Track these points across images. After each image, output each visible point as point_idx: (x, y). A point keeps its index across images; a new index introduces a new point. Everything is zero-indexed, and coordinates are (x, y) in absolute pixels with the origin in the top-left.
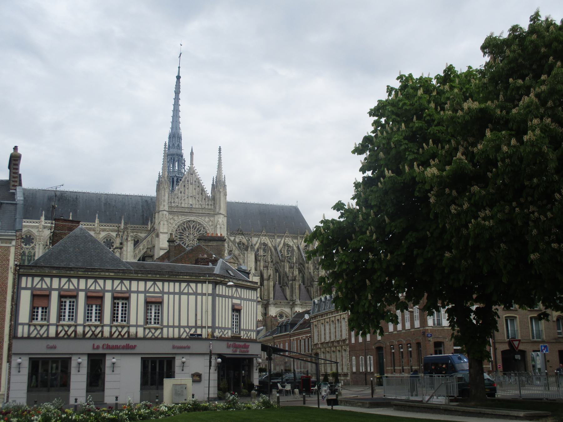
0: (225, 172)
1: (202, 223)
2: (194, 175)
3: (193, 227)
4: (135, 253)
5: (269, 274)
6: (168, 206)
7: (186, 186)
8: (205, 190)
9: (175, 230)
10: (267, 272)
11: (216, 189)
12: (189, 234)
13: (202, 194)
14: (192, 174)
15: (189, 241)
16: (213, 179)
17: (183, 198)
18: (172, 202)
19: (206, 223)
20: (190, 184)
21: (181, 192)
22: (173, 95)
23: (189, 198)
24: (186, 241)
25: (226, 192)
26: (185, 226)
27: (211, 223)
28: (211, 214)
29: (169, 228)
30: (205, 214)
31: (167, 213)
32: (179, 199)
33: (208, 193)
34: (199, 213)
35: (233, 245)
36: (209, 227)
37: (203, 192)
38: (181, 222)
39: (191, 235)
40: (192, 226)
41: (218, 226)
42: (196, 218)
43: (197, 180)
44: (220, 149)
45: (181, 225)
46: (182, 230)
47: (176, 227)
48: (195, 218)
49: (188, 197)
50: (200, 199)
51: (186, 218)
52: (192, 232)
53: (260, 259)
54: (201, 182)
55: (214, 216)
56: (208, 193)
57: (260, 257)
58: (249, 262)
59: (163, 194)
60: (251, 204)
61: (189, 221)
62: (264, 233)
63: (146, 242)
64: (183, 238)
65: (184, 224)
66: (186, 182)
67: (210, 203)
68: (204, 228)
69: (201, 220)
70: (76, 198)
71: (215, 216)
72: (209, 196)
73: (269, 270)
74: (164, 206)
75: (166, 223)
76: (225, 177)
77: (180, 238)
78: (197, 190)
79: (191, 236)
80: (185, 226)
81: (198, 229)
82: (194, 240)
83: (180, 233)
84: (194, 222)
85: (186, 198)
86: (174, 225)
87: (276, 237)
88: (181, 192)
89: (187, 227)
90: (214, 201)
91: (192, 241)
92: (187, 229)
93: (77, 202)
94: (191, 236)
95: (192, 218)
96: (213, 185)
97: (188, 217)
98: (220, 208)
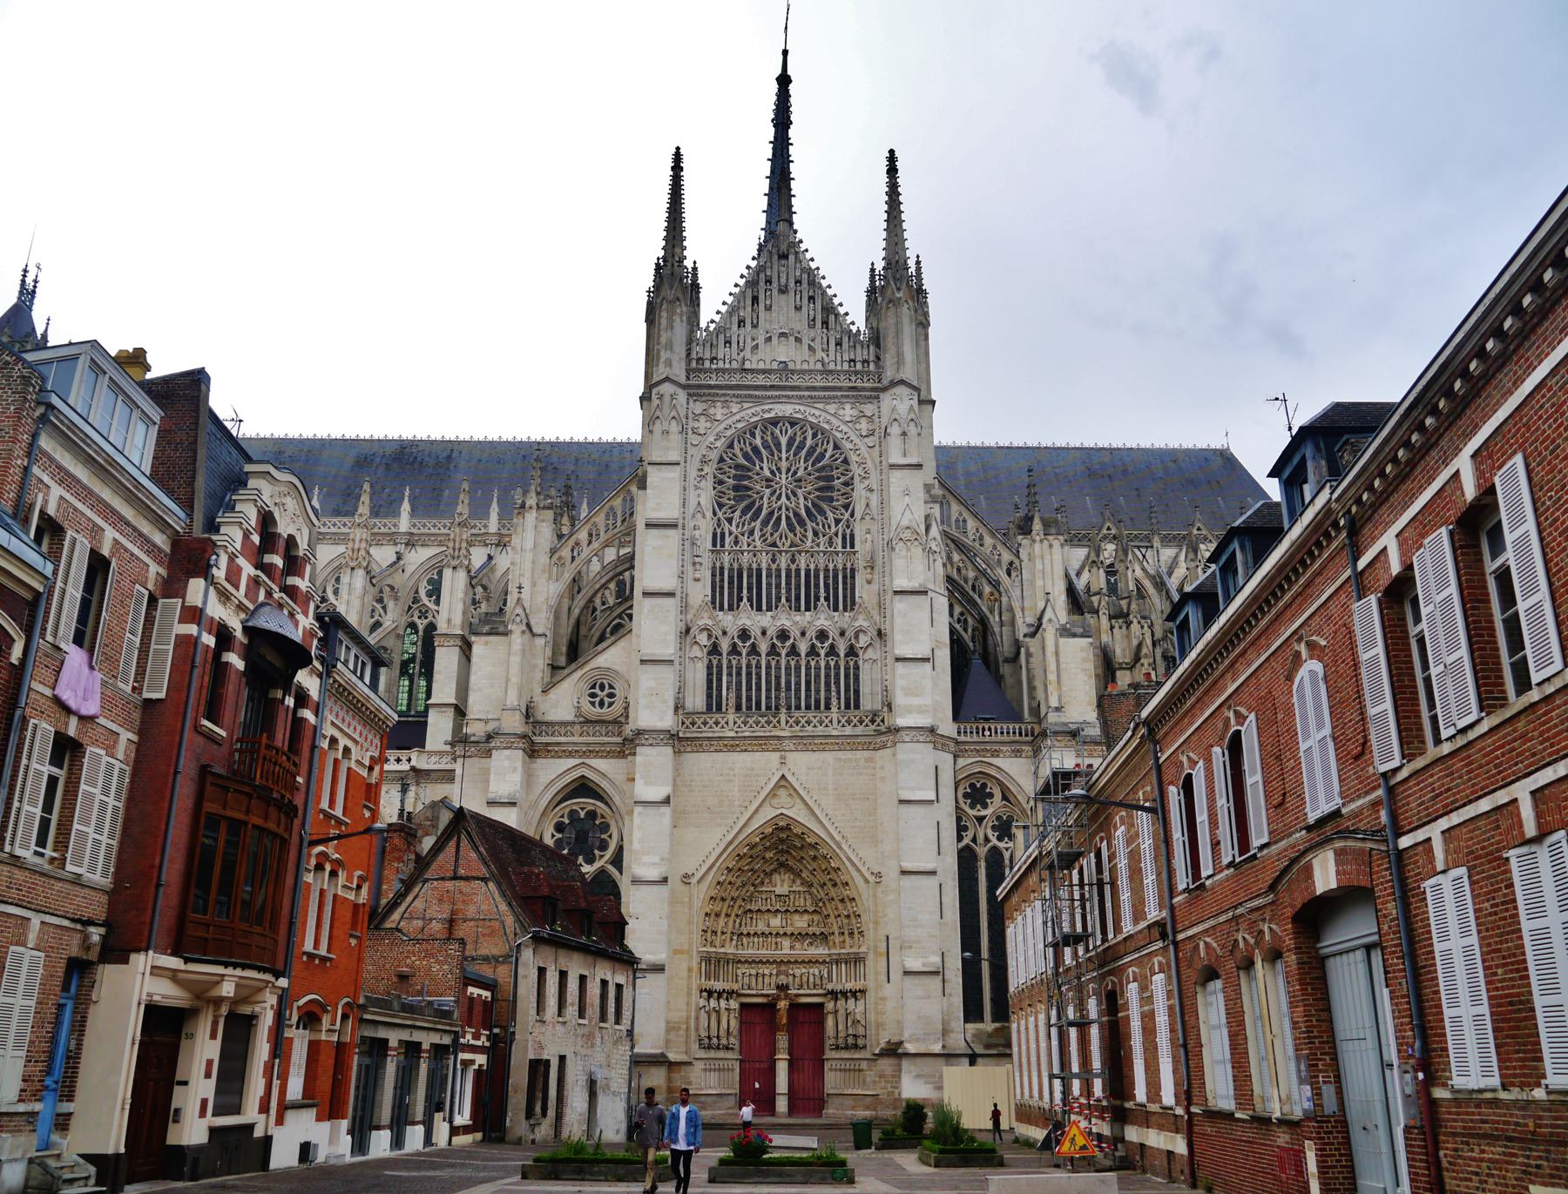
0: (914, 246)
1: (826, 426)
2: (792, 258)
3: (790, 444)
4: (556, 556)
5: (1135, 642)
6: (684, 367)
7: (761, 297)
8: (842, 310)
9: (714, 456)
10: (1128, 637)
11: (879, 300)
12: (772, 472)
13: (825, 323)
14: (784, 256)
15: (774, 498)
16: (873, 270)
17: (750, 344)
18: (707, 355)
19: (845, 429)
20: (775, 292)
21: (741, 323)
22: (770, 133)
23: (775, 340)
24: (762, 498)
25: (926, 315)
26: (758, 442)
27: (864, 426)
28: (864, 389)
29: (691, 451)
30: (840, 389)
31: (682, 396)
32: (734, 345)
33: (853, 323)
34: (814, 388)
35: (966, 515)
36: (857, 440)
37: (832, 318)
38: (740, 425)
39: (784, 476)
40: (784, 441)
41: (895, 430)
42: (802, 408)
43: (805, 276)
44: (892, 157)
45: (740, 437)
46: (746, 456)
47: (718, 444)
48: (797, 407)
49: (769, 339)
50: (817, 345)
51: (758, 409)
52: (784, 465)
53: (1096, 604)
54: (824, 283)
55: (878, 397)
56: (853, 323)
57: (1095, 599)
58: (1039, 575)
59: (664, 322)
60: (1054, 449)
61: (774, 422)
62: (1109, 529)
63: (602, 516)
64: (748, 488)
65: (753, 435)
66: (762, 284)
67: (860, 354)
68: (836, 447)
69: (824, 414)
70: (449, 457)
71: (882, 395)
72: (854, 329)
73: (1135, 627)
74: (669, 363)
75: (674, 427)
76: (918, 263)
77: (736, 488)
78: (805, 309)
79: (783, 479)
80: (758, 442)
81: (812, 449)
82: (795, 495)
83: (738, 467)
84: (793, 424)
85: (761, 340)
86: (712, 439)
87: (1156, 542)
88: (741, 323)
89: (765, 443)
90: (878, 346)
91: (788, 498)
92: (764, 452)
93: (448, 469)
94: (783, 479)
95: (786, 410)
96: (872, 292)
97: (766, 407)
98: (900, 362)
